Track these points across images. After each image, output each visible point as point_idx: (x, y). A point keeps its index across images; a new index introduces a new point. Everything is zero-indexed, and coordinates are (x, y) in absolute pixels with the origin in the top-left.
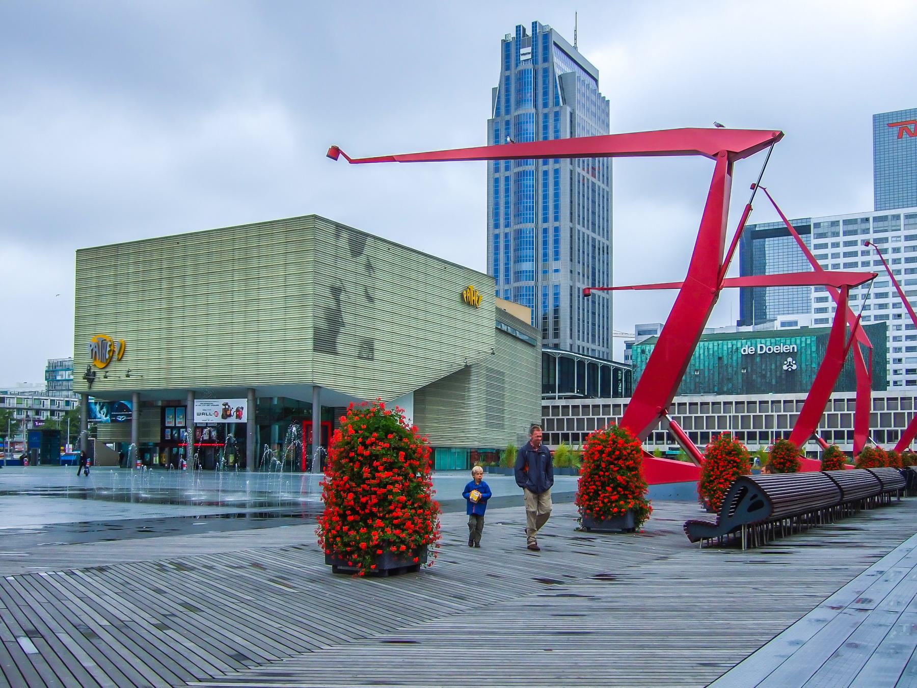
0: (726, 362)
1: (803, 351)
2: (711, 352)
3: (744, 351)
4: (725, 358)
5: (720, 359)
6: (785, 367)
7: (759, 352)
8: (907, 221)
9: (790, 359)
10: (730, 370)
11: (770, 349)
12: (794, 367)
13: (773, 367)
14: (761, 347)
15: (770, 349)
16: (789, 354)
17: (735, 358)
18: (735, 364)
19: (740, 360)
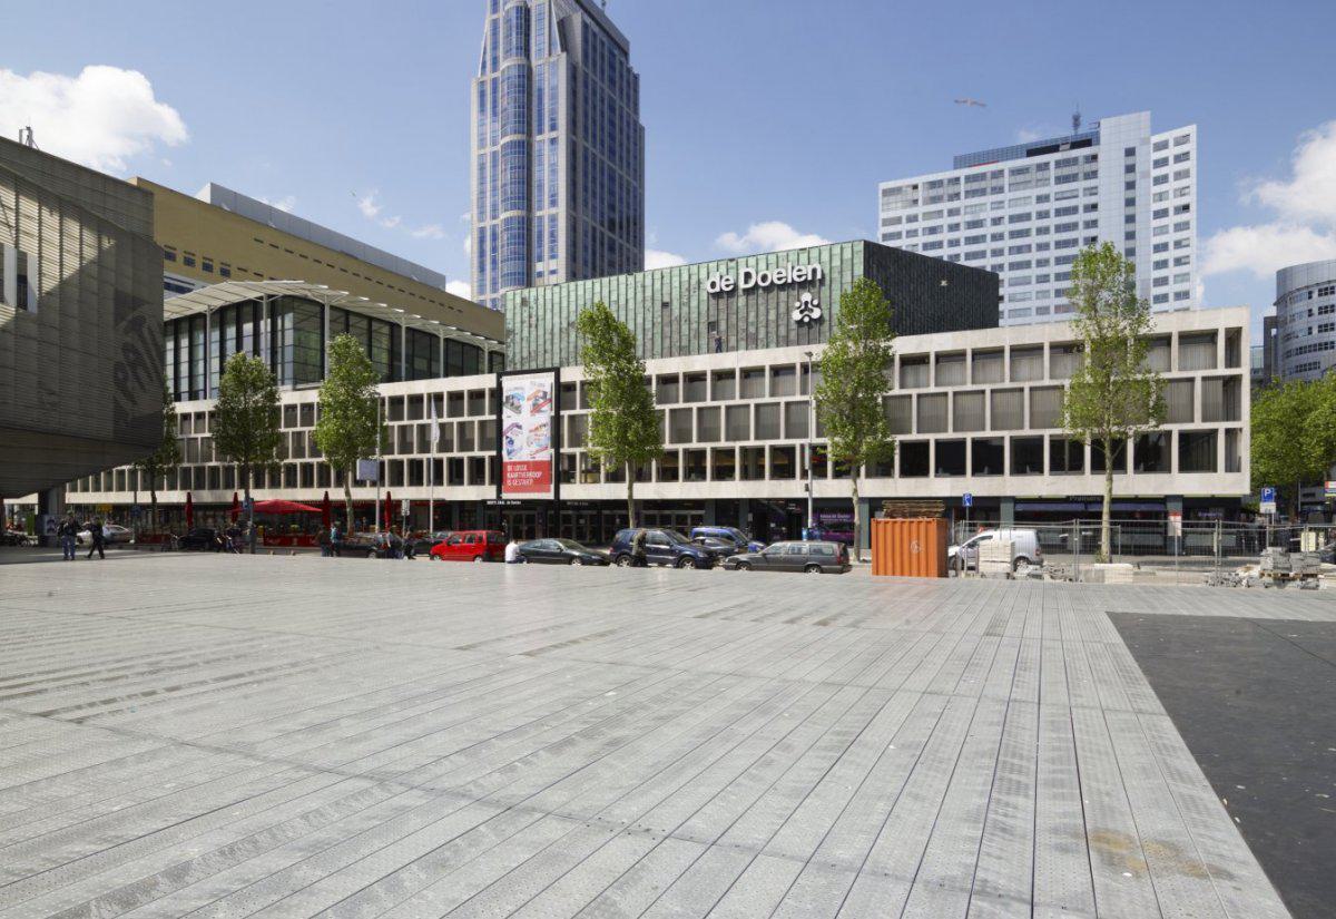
0: (676, 312)
1: (836, 275)
2: (649, 293)
3: (713, 285)
4: (676, 304)
5: (665, 305)
6: (796, 316)
7: (742, 285)
8: (1013, 179)
9: (806, 297)
10: (685, 328)
11: (764, 278)
12: (816, 314)
13: (772, 316)
14: (748, 276)
15: (764, 278)
16: (805, 285)
17: (694, 303)
18: (694, 316)
19: (704, 307)
